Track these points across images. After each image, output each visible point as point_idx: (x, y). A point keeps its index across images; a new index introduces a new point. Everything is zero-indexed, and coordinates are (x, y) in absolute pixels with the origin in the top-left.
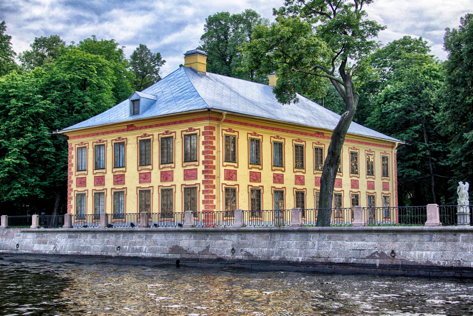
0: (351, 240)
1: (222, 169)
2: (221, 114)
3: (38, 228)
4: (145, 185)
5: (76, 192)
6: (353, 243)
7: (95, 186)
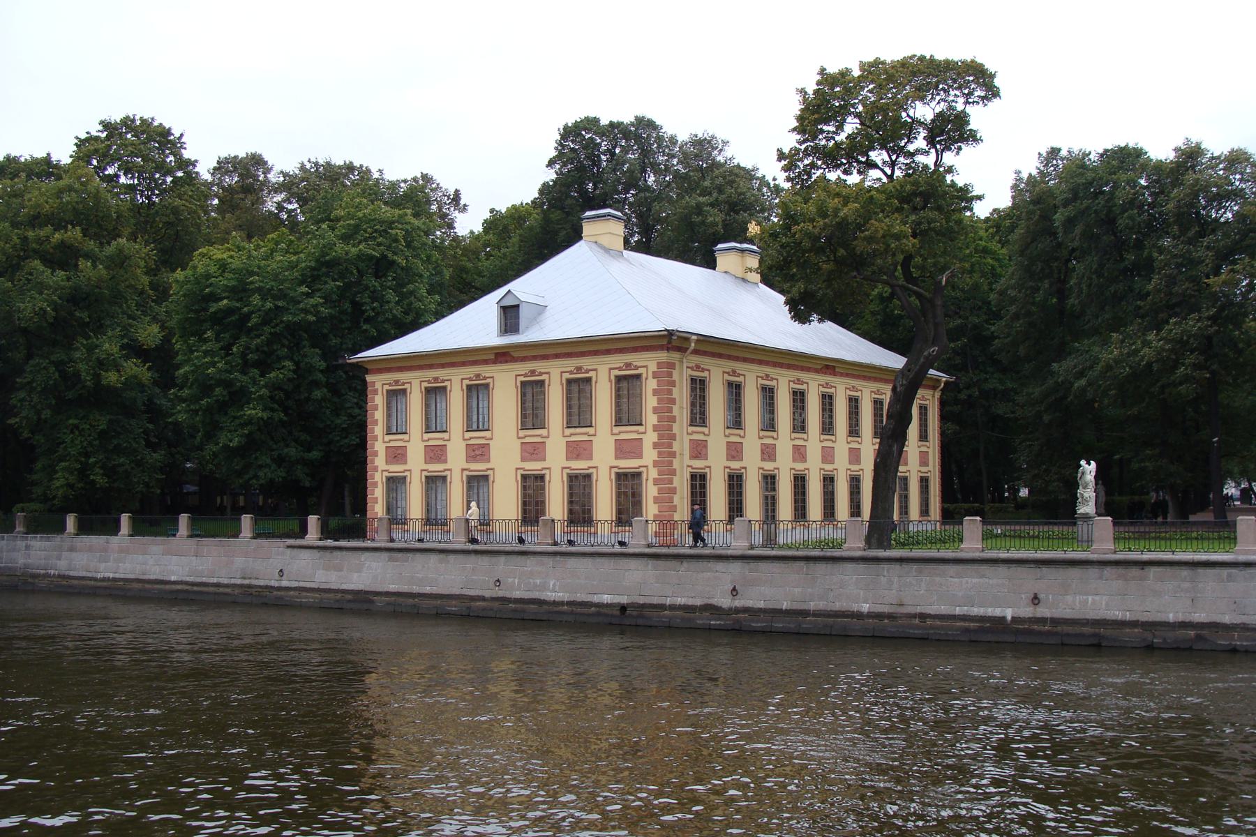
0: (959, 576)
1: (687, 439)
2: (687, 339)
3: (320, 540)
4: (533, 466)
5: (386, 474)
6: (964, 580)
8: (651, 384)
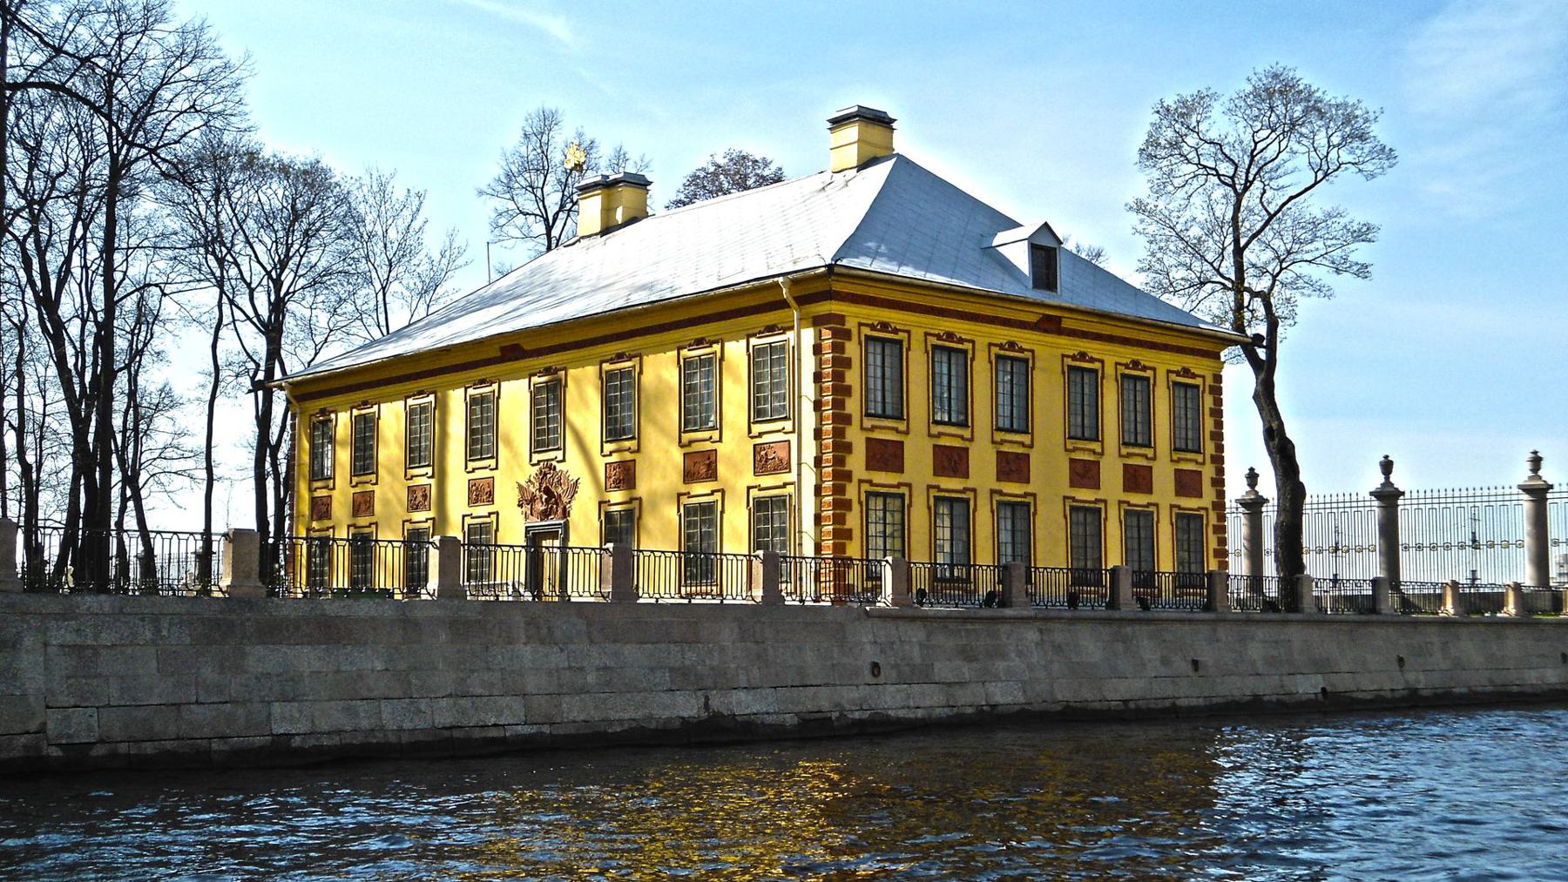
4: (1085, 495)
5: (865, 487)
7: (935, 474)
8: (1208, 401)
